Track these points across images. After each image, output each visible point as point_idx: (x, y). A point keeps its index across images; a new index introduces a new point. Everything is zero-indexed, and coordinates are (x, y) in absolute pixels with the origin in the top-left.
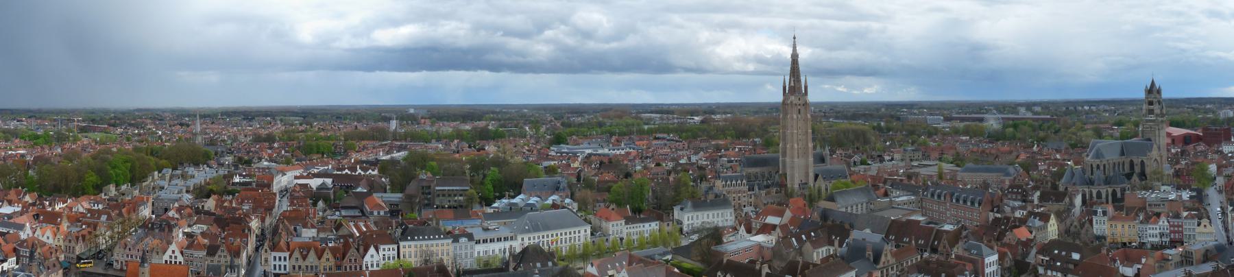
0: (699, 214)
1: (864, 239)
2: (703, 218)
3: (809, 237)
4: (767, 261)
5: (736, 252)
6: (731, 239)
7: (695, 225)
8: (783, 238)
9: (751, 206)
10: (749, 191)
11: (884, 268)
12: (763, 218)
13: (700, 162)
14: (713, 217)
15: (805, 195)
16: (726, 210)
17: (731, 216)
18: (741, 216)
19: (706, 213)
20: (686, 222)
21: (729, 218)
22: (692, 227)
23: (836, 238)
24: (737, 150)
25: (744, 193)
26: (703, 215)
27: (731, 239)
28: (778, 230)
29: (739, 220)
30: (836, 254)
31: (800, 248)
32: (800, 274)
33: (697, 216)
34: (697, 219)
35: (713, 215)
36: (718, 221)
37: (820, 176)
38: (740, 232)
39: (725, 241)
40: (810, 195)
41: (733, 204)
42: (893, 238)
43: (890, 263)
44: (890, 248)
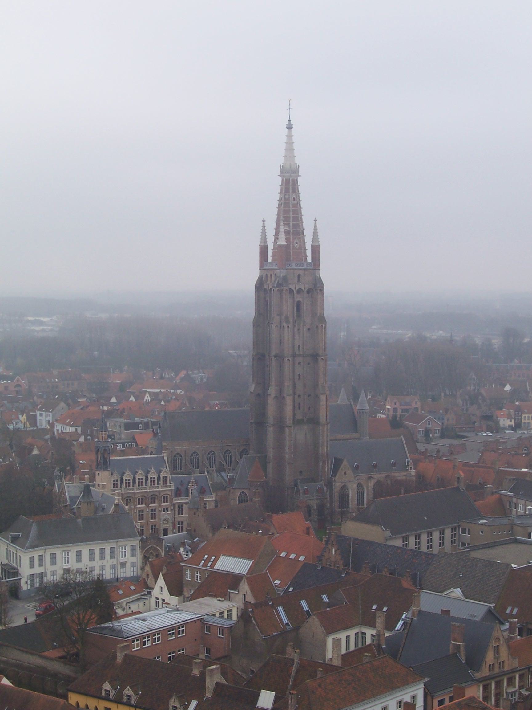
0: (59, 551)
1: (446, 613)
2: (67, 561)
3: (315, 604)
4: (219, 659)
5: (142, 638)
6: (134, 607)
7: (49, 578)
8: (255, 606)
9: (180, 530)
10: (178, 494)
11: (493, 678)
12: (207, 561)
13: (58, 427)
14: (92, 558)
15: (309, 508)
16: (122, 542)
17: (133, 555)
18: (157, 556)
19: (73, 550)
20: (25, 571)
21: (129, 559)
22: (41, 584)
23: (380, 608)
24: (147, 398)
25: (165, 500)
26: (67, 553)
27: (134, 607)
28: (245, 587)
29: (152, 567)
30: (379, 646)
31: (297, 629)
32: (293, 688)
33: (53, 556)
34: (53, 563)
35: (92, 553)
36: (103, 568)
37: (345, 463)
38: (156, 592)
39: (120, 612)
40: (321, 508)
41: (138, 525)
42: (515, 612)
43: (506, 669)
44: (506, 634)
